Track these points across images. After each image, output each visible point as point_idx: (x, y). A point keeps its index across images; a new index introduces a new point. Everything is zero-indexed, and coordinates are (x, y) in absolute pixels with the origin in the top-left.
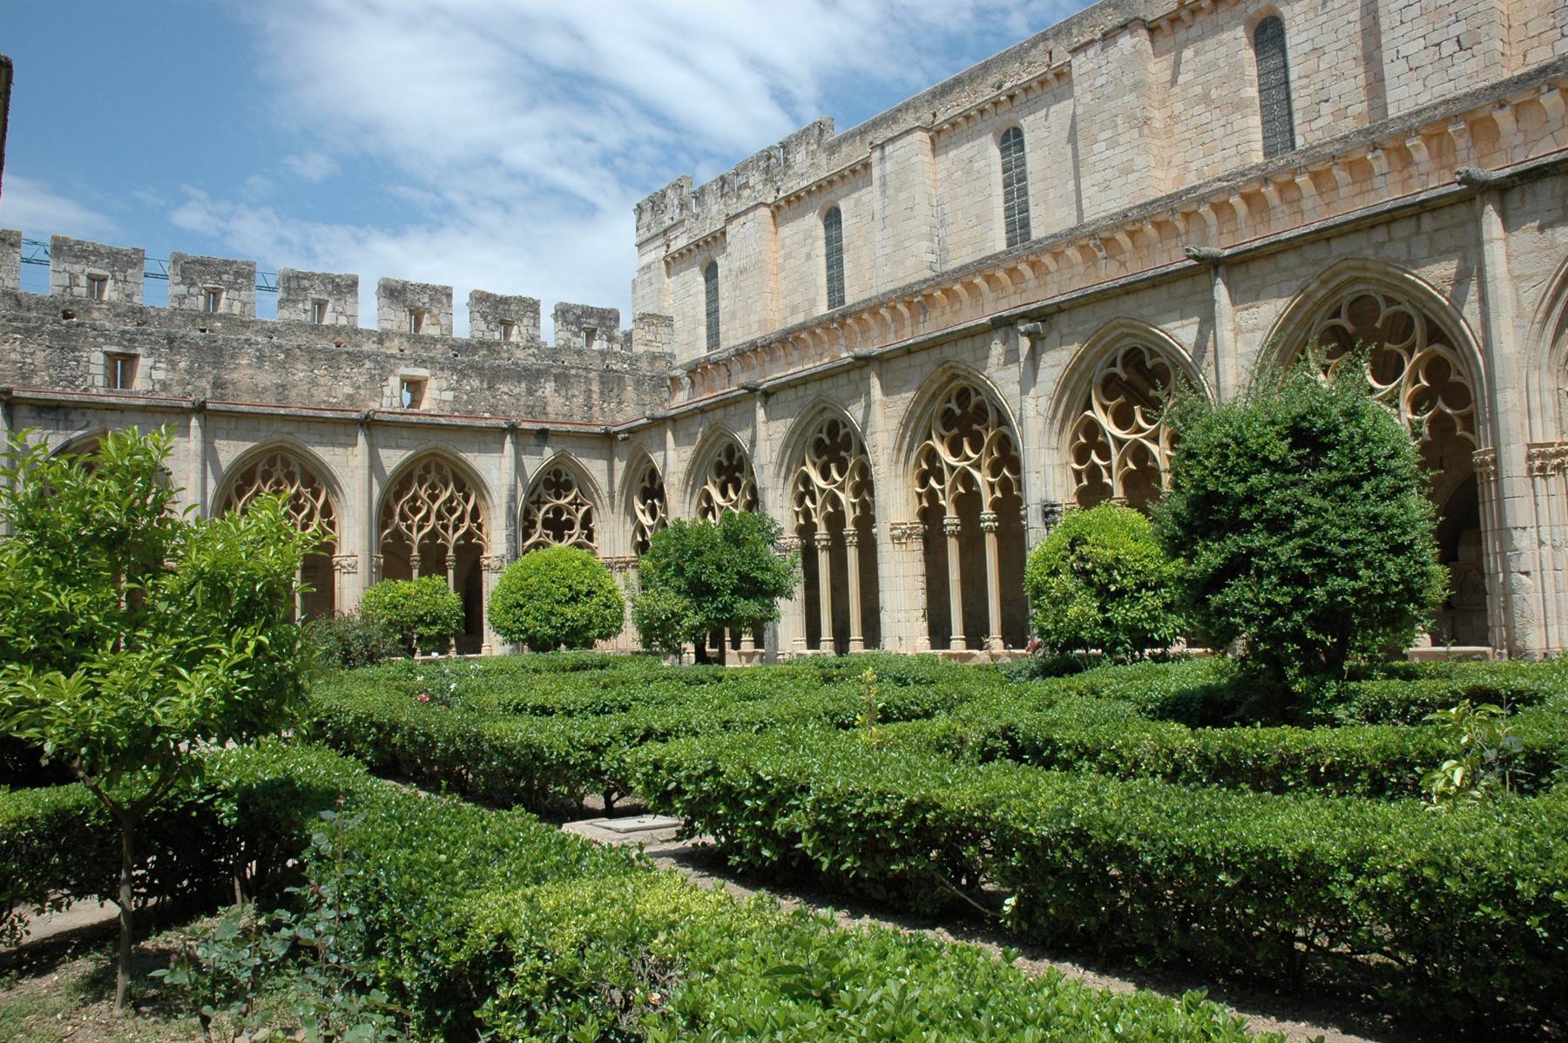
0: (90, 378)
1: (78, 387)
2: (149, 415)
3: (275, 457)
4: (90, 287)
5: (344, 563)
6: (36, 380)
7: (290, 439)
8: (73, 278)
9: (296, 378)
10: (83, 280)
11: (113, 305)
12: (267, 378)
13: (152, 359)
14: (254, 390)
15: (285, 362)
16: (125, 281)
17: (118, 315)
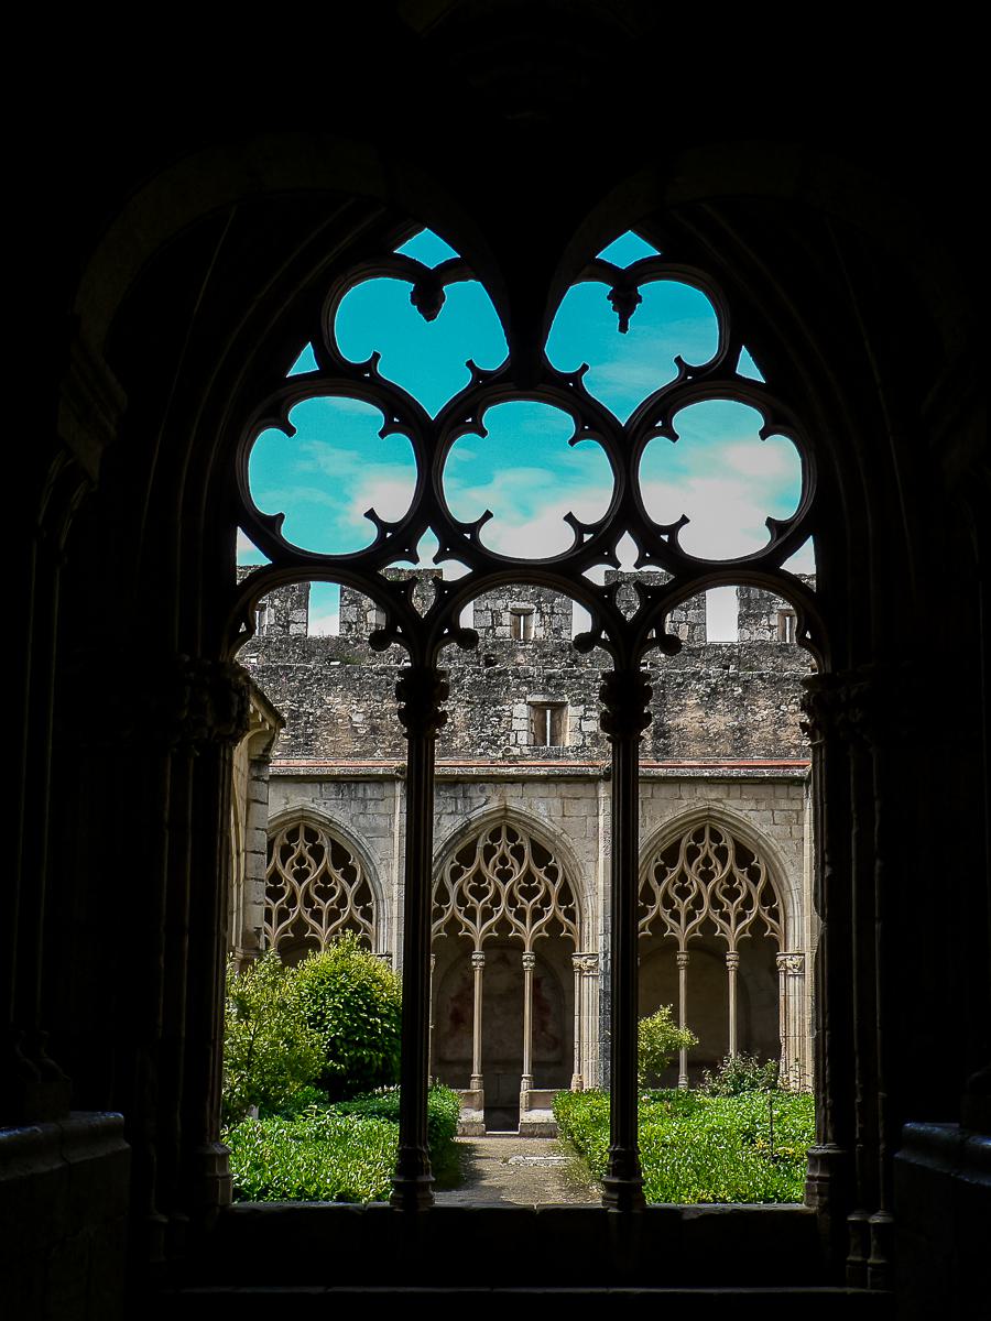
0: (512, 734)
1: (499, 747)
2: (552, 785)
3: (703, 829)
4: (516, 625)
5: (789, 964)
6: (457, 743)
7: (719, 806)
8: (496, 615)
9: (758, 717)
10: (507, 618)
11: (539, 644)
12: (721, 721)
13: (582, 707)
14: (705, 738)
15: (742, 699)
16: (553, 613)
17: (545, 656)
